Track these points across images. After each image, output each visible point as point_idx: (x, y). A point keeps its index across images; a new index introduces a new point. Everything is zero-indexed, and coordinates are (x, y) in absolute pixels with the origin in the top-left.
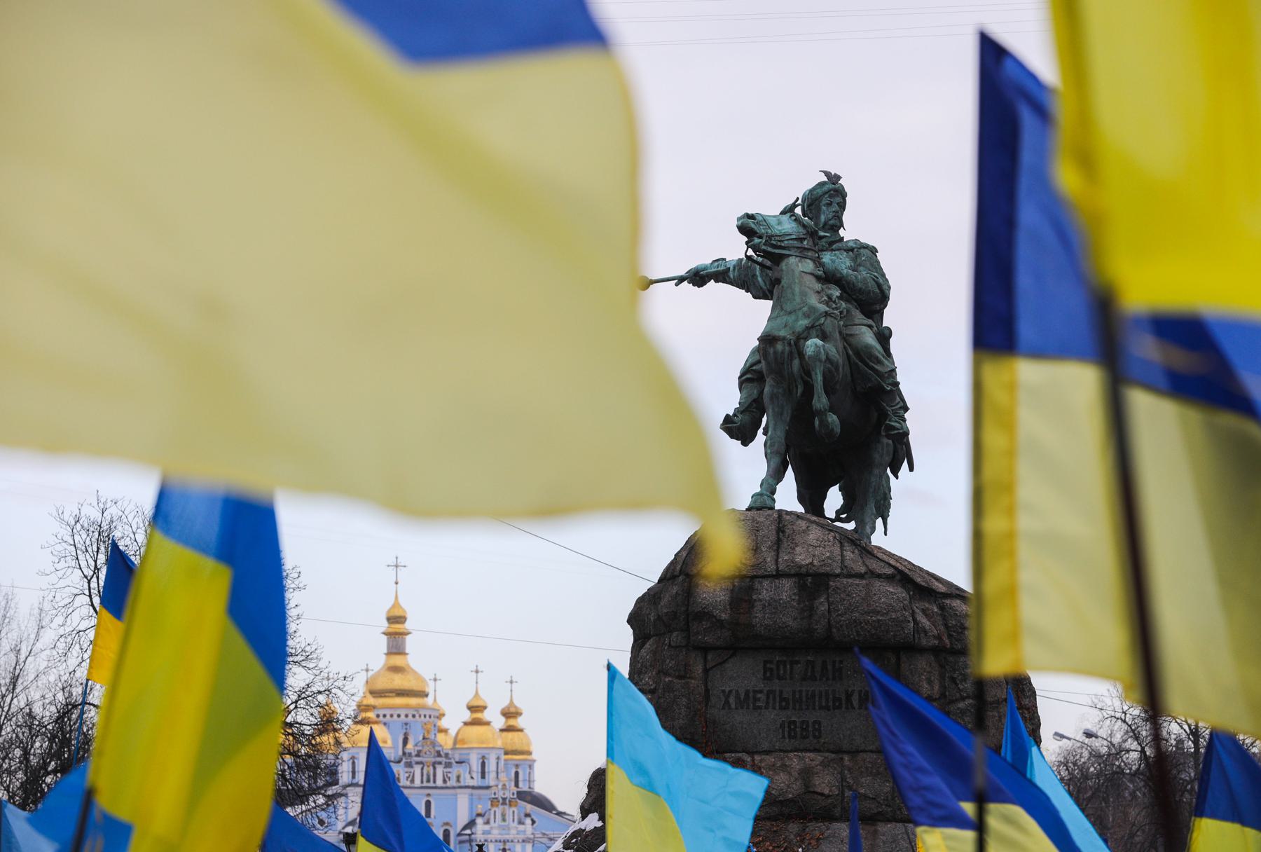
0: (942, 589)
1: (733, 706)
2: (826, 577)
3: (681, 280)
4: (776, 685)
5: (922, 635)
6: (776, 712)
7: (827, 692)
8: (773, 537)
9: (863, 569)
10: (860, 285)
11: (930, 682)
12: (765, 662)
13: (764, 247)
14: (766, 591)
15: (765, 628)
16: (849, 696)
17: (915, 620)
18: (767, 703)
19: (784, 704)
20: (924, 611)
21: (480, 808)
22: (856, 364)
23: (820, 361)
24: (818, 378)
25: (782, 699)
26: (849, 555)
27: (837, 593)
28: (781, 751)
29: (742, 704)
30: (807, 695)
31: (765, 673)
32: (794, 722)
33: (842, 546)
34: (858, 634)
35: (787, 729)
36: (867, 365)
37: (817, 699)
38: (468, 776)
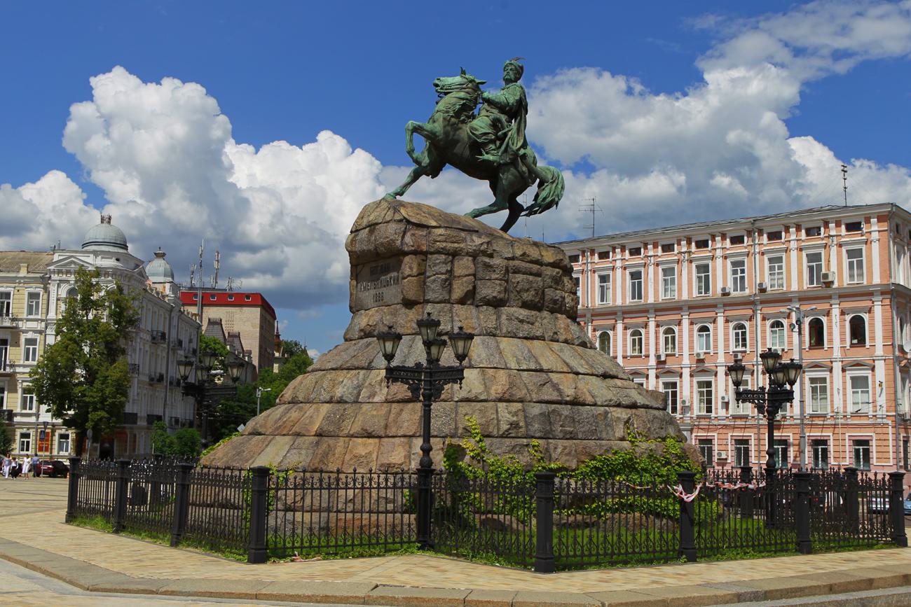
2: (377, 224)
11: (411, 268)
16: (391, 279)
20: (413, 235)
23: (409, 130)
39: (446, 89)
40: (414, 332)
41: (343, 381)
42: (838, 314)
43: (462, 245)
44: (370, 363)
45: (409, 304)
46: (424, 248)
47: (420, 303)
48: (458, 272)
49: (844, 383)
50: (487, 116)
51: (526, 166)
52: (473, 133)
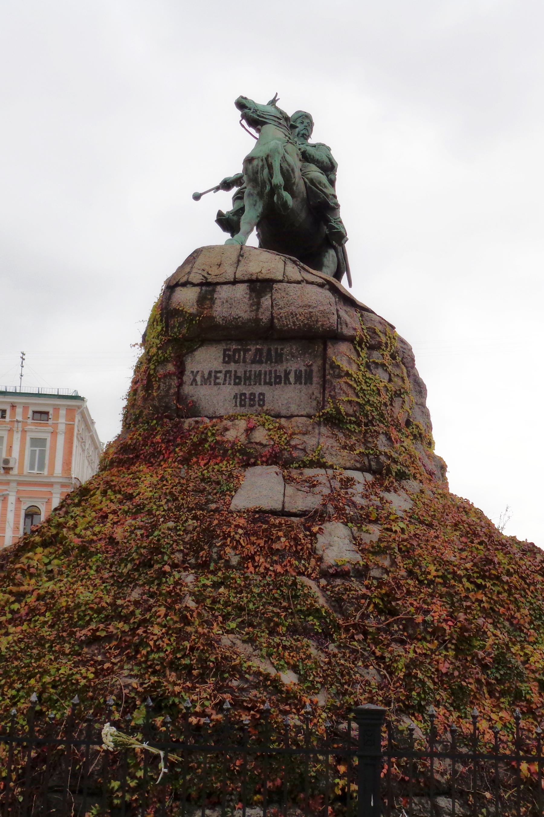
1: (199, 383)
3: (217, 189)
4: (232, 367)
5: (344, 326)
6: (231, 387)
7: (270, 371)
8: (234, 258)
9: (300, 279)
12: (225, 351)
14: (223, 292)
15: (223, 320)
16: (287, 374)
17: (339, 317)
18: (225, 380)
19: (237, 381)
22: (310, 188)
25: (236, 377)
29: (206, 381)
30: (255, 373)
31: (224, 358)
32: (245, 394)
36: (317, 188)
37: (262, 377)
40: (358, 465)
42: (14, 502)
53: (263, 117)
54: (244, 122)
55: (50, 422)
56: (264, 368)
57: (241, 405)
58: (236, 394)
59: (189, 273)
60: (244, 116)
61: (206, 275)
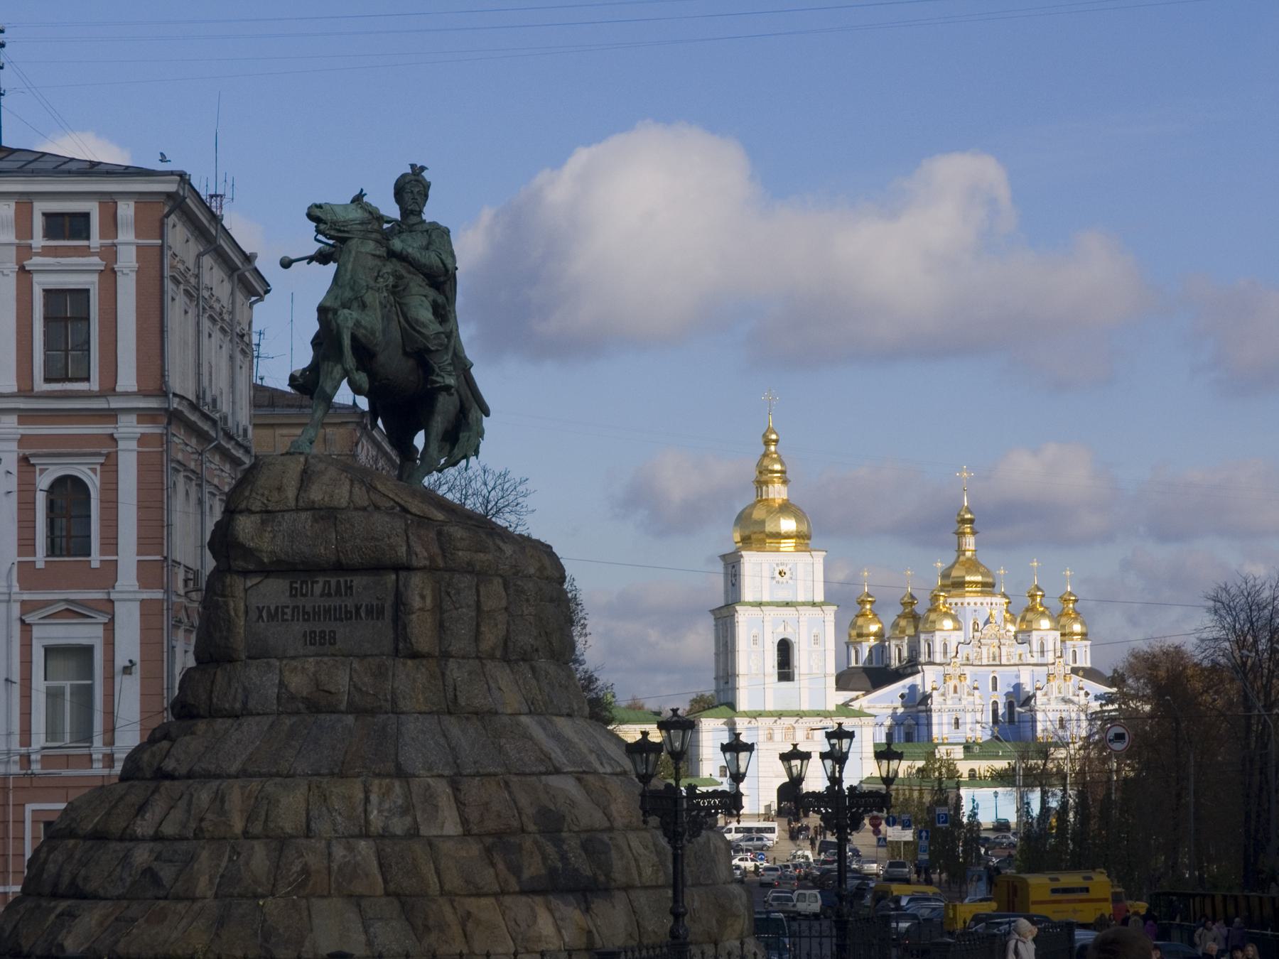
0: (440, 516)
1: (265, 619)
2: (336, 509)
3: (311, 259)
4: (301, 601)
5: (414, 557)
9: (366, 504)
10: (423, 260)
11: (423, 597)
12: (291, 583)
13: (328, 232)
16: (358, 609)
17: (409, 546)
18: (293, 616)
21: (1039, 685)
23: (348, 328)
24: (347, 342)
25: (308, 613)
26: (356, 490)
27: (342, 524)
28: (306, 656)
29: (272, 617)
30: (324, 610)
33: (352, 481)
34: (362, 559)
35: (308, 639)
38: (1029, 655)
39: (340, 231)
40: (435, 709)
41: (367, 800)
42: (14, 470)
43: (490, 557)
44: (398, 766)
45: (415, 655)
46: (441, 563)
47: (432, 657)
48: (488, 605)
49: (27, 663)
50: (425, 296)
51: (471, 390)
52: (419, 332)
53: (344, 231)
54: (320, 237)
55: (95, 241)
56: (335, 602)
57: (311, 644)
58: (306, 632)
59: (248, 498)
60: (318, 231)
61: (266, 502)
